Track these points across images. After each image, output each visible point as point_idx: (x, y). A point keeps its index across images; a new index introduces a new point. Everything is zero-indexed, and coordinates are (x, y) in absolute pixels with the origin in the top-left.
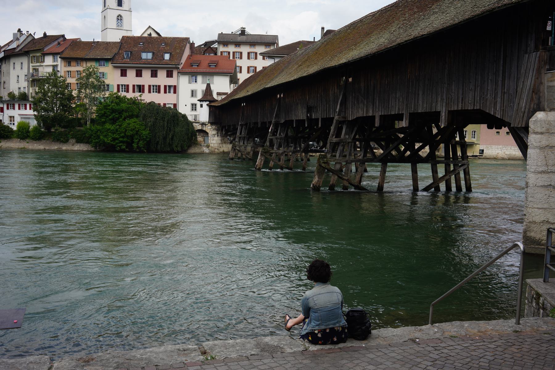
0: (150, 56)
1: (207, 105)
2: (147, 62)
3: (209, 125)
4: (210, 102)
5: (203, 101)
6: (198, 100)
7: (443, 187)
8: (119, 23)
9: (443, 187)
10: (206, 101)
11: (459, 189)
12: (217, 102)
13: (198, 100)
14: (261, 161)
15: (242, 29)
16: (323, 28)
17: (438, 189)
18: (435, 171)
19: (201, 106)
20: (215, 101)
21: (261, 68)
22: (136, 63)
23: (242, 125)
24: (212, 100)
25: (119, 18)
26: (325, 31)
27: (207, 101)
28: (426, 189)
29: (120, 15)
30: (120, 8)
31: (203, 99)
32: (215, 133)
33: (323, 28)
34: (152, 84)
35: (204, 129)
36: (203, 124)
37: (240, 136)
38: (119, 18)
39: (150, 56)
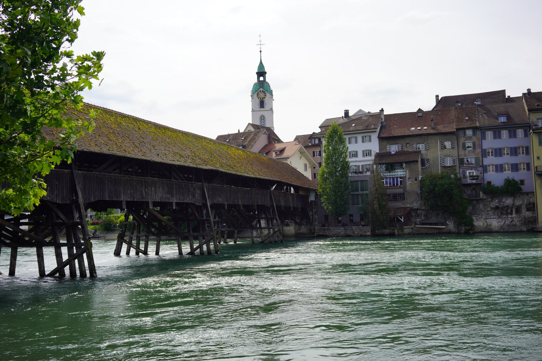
7: (67, 270)
8: (263, 123)
9: (67, 270)
11: (83, 274)
14: (119, 246)
15: (346, 111)
16: (437, 96)
17: (63, 274)
18: (59, 255)
21: (60, 162)
25: (262, 118)
26: (440, 98)
28: (52, 274)
29: (262, 115)
30: (262, 109)
33: (437, 96)
38: (262, 118)
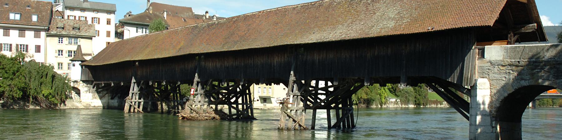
0: (18, 17)
1: (80, 64)
2: (15, 22)
3: (81, 82)
4: (82, 61)
5: (75, 61)
6: (70, 60)
10: (78, 61)
12: (87, 62)
13: (70, 60)
19: (74, 65)
20: (85, 61)
22: (4, 22)
23: (135, 83)
24: (84, 60)
27: (80, 61)
31: (73, 59)
32: (87, 90)
34: (19, 43)
35: (76, 86)
36: (76, 82)
37: (133, 92)
39: (18, 17)
